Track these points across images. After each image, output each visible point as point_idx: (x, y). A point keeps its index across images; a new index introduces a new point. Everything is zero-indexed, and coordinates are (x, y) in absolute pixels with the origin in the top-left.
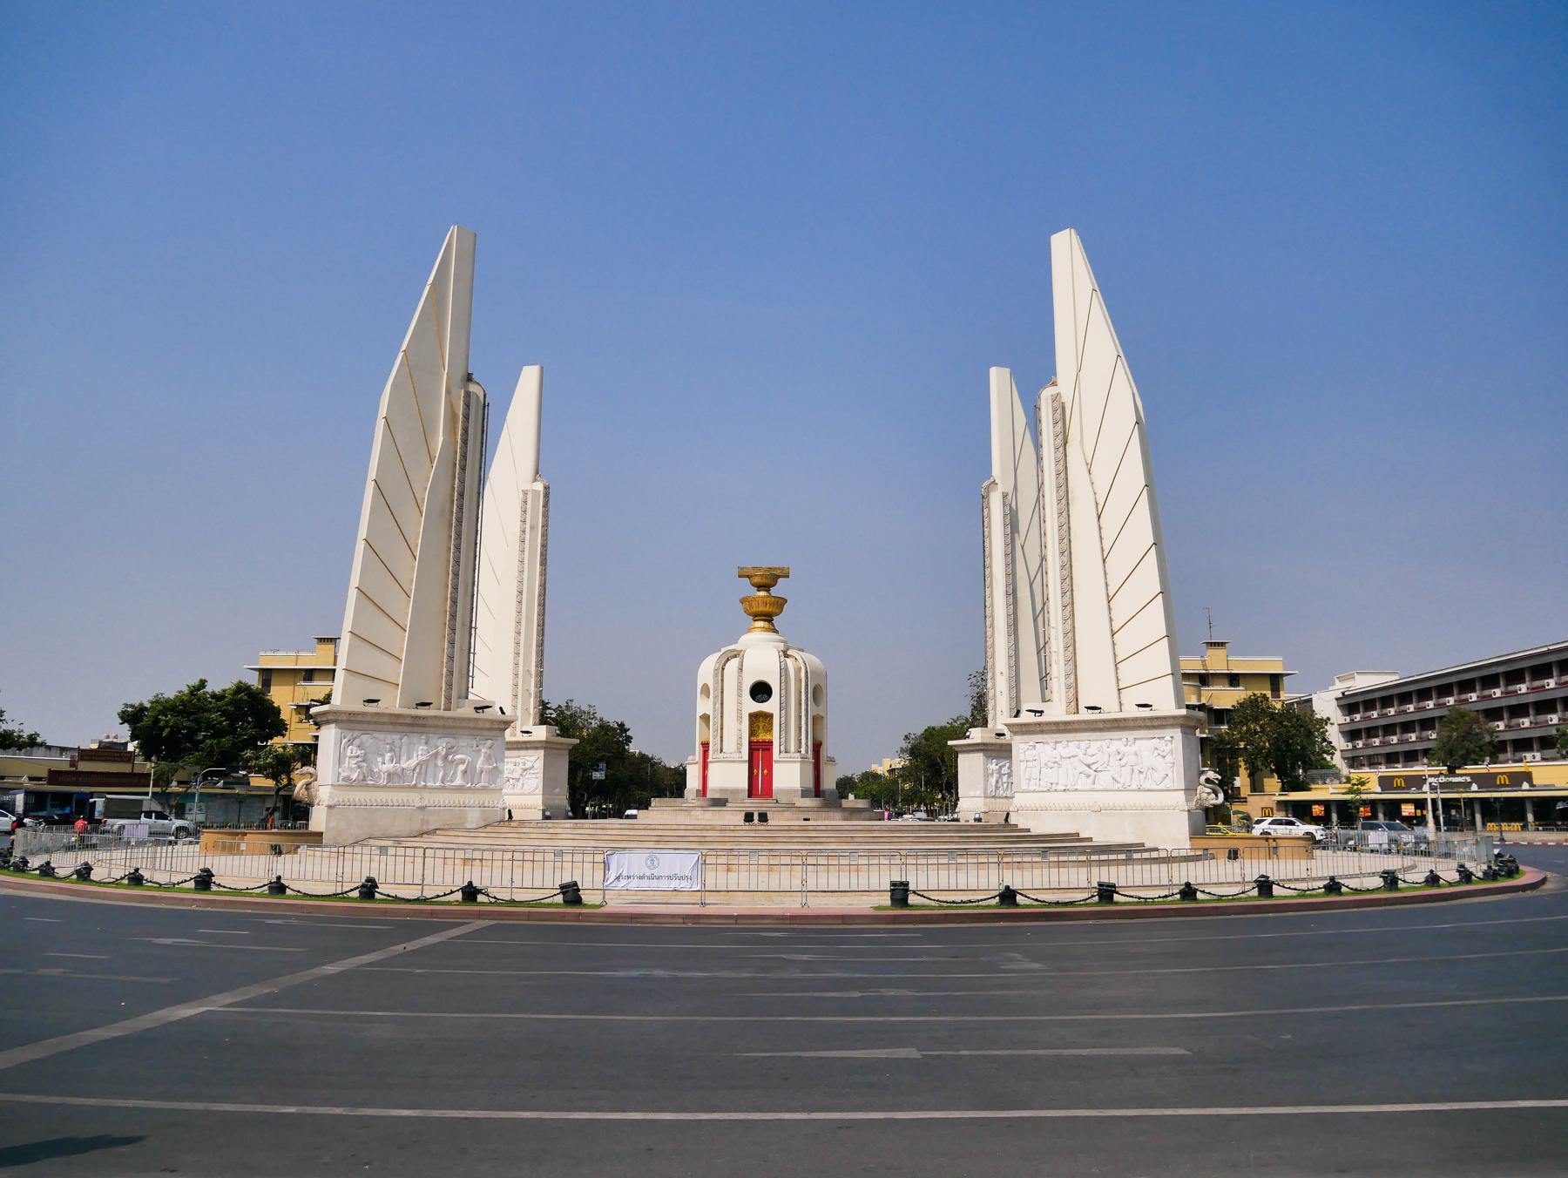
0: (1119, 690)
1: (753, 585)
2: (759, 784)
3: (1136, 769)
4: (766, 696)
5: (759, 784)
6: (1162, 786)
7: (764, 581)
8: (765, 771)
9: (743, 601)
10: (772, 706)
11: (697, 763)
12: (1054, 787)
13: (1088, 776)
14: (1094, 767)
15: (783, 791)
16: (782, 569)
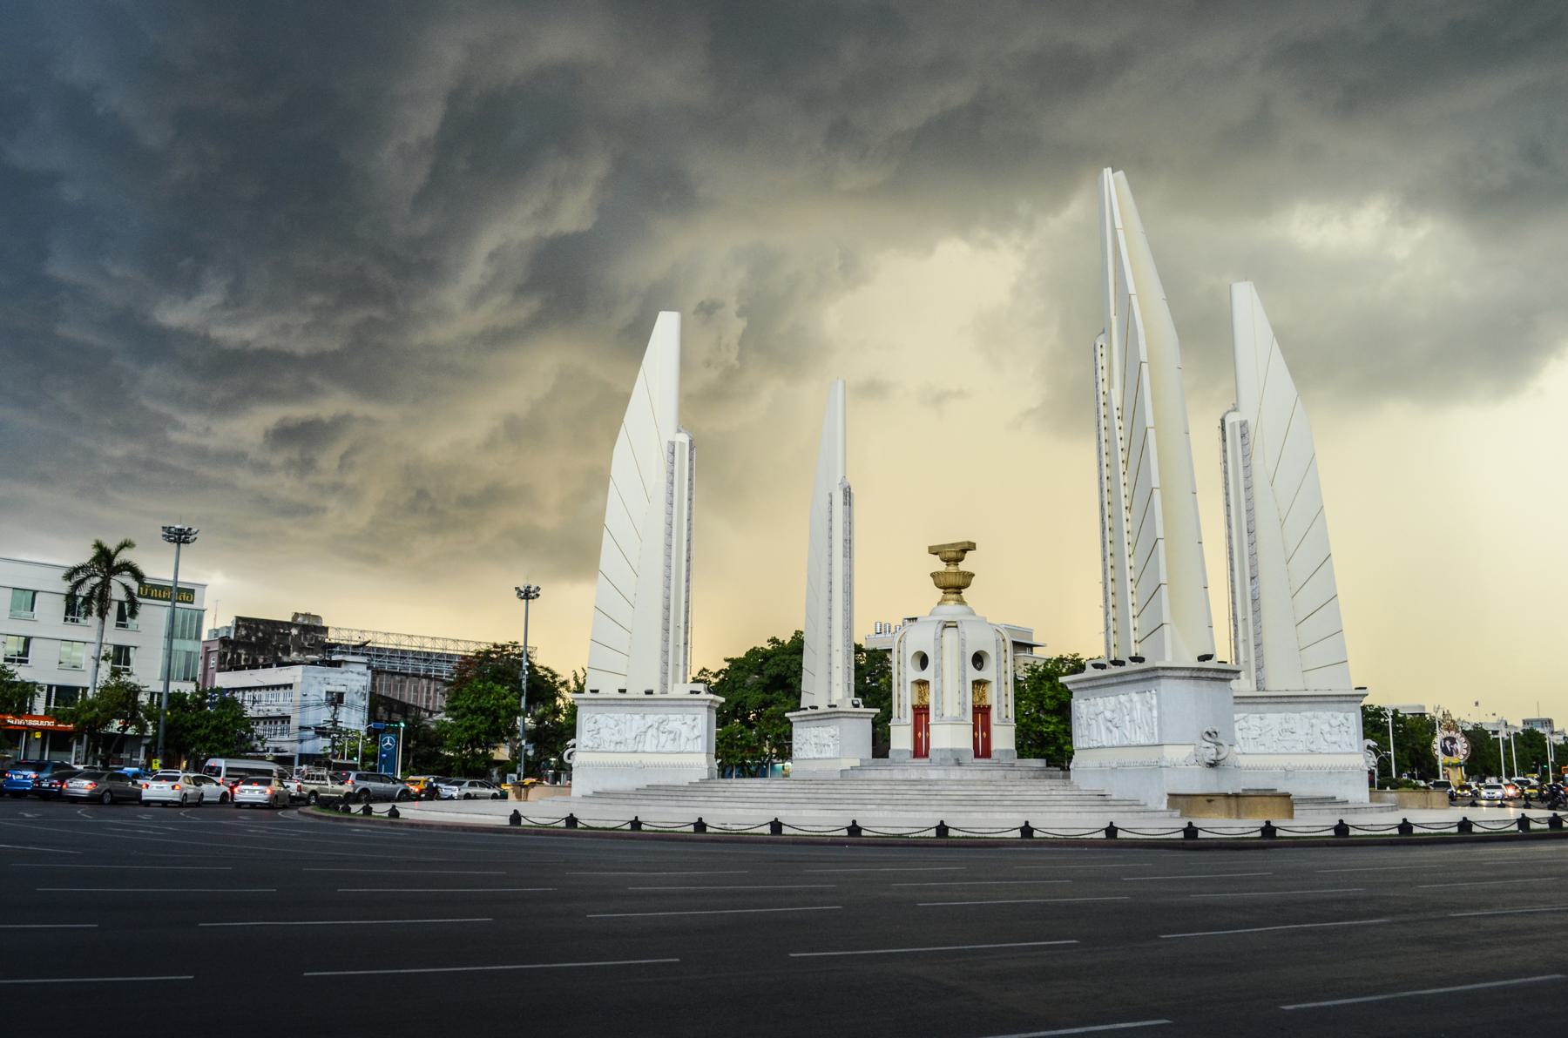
1: (942, 560)
2: (982, 749)
5: (982, 749)
7: (953, 555)
8: (985, 734)
9: (933, 575)
10: (988, 673)
16: (969, 543)
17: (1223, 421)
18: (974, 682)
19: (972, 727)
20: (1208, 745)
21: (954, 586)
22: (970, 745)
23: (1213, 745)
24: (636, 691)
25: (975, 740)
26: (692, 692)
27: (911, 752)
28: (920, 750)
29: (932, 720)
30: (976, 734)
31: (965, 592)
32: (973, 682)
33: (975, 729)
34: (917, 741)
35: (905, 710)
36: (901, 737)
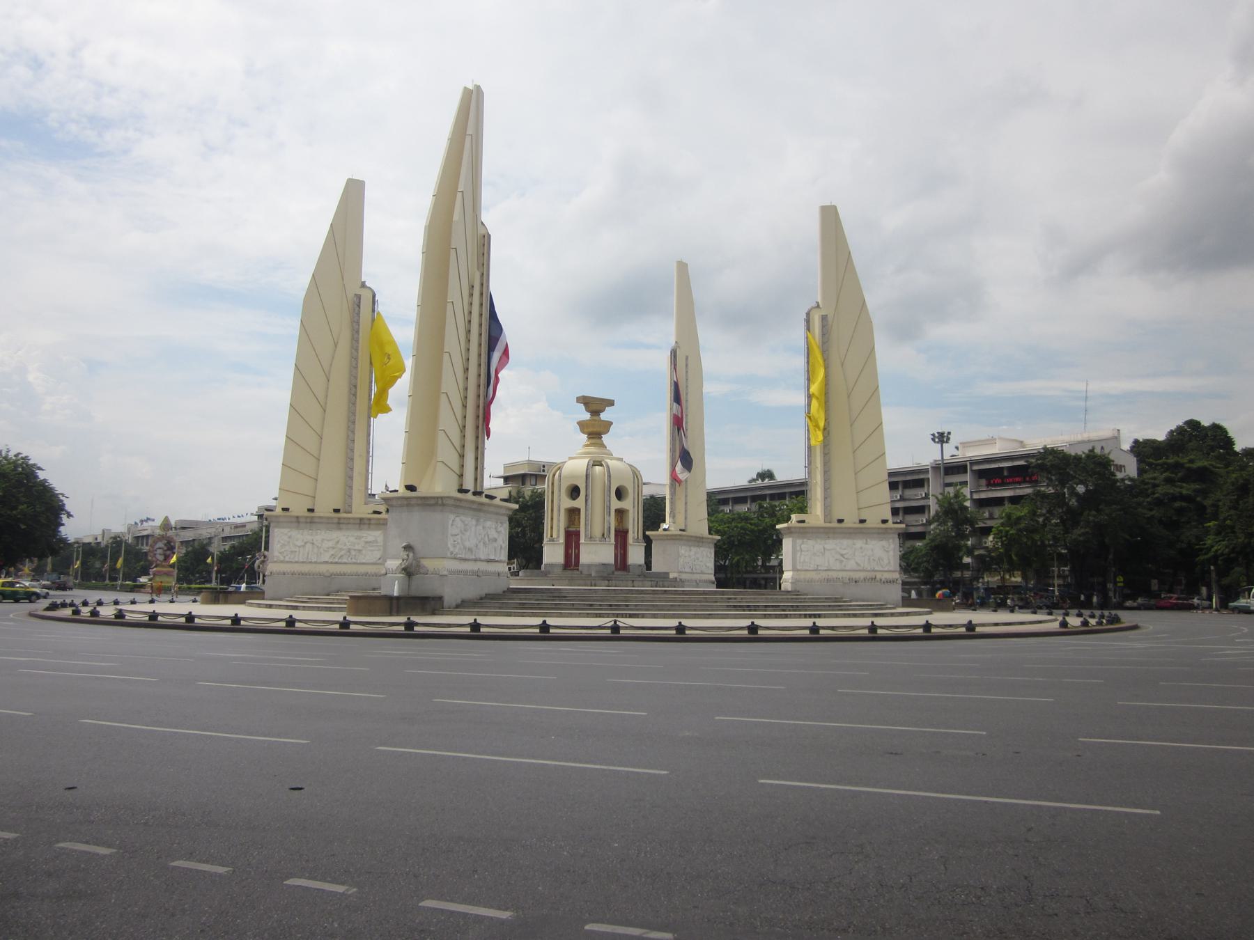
0: (859, 509)
2: (622, 562)
3: (872, 558)
4: (576, 494)
6: (886, 569)
8: (622, 552)
9: (578, 423)
10: (627, 504)
12: (819, 568)
13: (841, 561)
14: (846, 556)
17: (808, 314)
21: (595, 431)
22: (612, 561)
24: (324, 509)
26: (375, 512)
28: (571, 561)
29: (582, 541)
31: (605, 438)
32: (616, 510)
34: (567, 556)
35: (559, 531)
36: (553, 553)
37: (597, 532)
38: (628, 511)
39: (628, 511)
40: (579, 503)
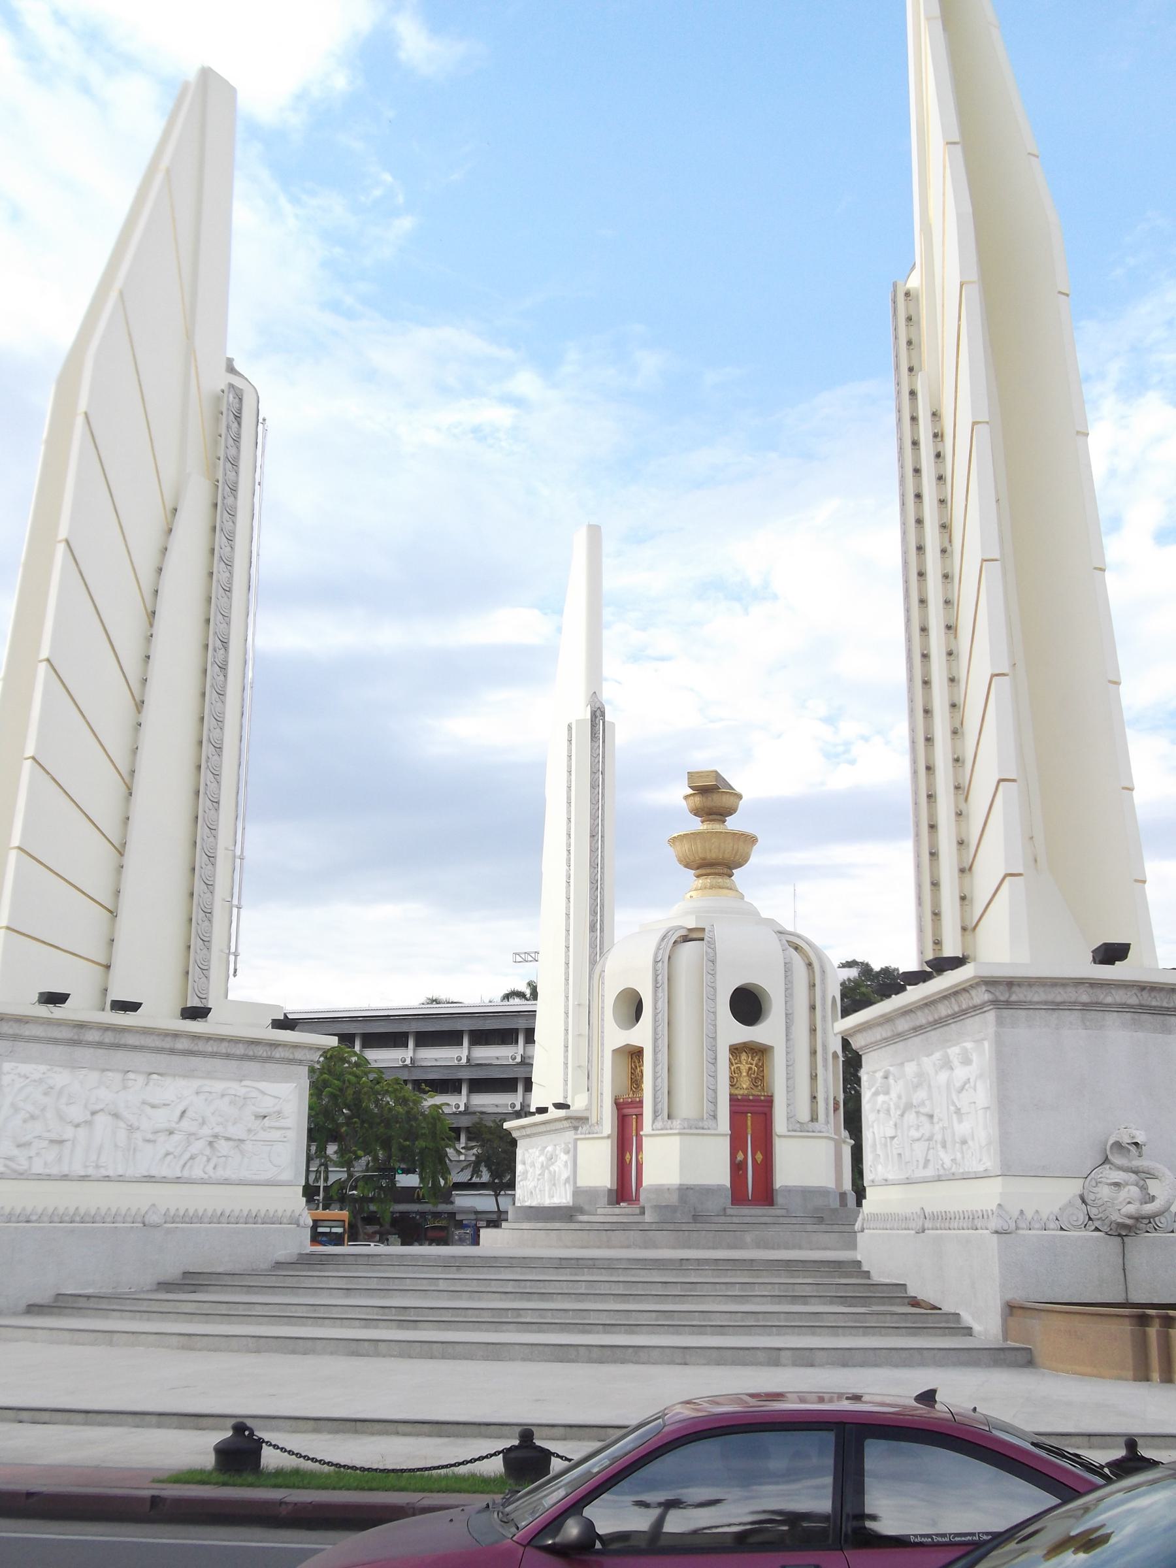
8: (759, 1157)
11: (608, 1137)
15: (789, 1190)
18: (735, 1050)
19: (729, 1137)
20: (1118, 1176)
23: (1133, 1177)
25: (737, 1169)
27: (610, 1191)
30: (740, 1157)
33: (737, 1142)
34: (623, 1169)
37: (687, 1103)
38: (771, 1048)
39: (771, 1048)
40: (641, 1035)
